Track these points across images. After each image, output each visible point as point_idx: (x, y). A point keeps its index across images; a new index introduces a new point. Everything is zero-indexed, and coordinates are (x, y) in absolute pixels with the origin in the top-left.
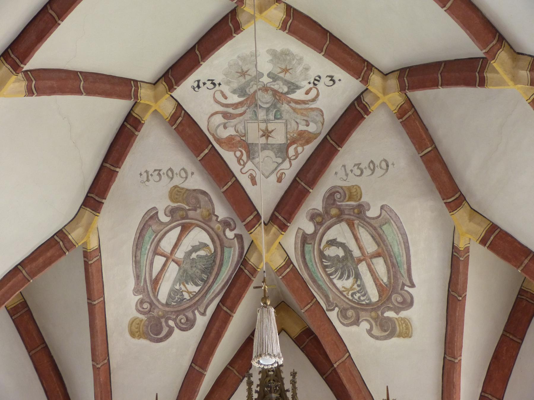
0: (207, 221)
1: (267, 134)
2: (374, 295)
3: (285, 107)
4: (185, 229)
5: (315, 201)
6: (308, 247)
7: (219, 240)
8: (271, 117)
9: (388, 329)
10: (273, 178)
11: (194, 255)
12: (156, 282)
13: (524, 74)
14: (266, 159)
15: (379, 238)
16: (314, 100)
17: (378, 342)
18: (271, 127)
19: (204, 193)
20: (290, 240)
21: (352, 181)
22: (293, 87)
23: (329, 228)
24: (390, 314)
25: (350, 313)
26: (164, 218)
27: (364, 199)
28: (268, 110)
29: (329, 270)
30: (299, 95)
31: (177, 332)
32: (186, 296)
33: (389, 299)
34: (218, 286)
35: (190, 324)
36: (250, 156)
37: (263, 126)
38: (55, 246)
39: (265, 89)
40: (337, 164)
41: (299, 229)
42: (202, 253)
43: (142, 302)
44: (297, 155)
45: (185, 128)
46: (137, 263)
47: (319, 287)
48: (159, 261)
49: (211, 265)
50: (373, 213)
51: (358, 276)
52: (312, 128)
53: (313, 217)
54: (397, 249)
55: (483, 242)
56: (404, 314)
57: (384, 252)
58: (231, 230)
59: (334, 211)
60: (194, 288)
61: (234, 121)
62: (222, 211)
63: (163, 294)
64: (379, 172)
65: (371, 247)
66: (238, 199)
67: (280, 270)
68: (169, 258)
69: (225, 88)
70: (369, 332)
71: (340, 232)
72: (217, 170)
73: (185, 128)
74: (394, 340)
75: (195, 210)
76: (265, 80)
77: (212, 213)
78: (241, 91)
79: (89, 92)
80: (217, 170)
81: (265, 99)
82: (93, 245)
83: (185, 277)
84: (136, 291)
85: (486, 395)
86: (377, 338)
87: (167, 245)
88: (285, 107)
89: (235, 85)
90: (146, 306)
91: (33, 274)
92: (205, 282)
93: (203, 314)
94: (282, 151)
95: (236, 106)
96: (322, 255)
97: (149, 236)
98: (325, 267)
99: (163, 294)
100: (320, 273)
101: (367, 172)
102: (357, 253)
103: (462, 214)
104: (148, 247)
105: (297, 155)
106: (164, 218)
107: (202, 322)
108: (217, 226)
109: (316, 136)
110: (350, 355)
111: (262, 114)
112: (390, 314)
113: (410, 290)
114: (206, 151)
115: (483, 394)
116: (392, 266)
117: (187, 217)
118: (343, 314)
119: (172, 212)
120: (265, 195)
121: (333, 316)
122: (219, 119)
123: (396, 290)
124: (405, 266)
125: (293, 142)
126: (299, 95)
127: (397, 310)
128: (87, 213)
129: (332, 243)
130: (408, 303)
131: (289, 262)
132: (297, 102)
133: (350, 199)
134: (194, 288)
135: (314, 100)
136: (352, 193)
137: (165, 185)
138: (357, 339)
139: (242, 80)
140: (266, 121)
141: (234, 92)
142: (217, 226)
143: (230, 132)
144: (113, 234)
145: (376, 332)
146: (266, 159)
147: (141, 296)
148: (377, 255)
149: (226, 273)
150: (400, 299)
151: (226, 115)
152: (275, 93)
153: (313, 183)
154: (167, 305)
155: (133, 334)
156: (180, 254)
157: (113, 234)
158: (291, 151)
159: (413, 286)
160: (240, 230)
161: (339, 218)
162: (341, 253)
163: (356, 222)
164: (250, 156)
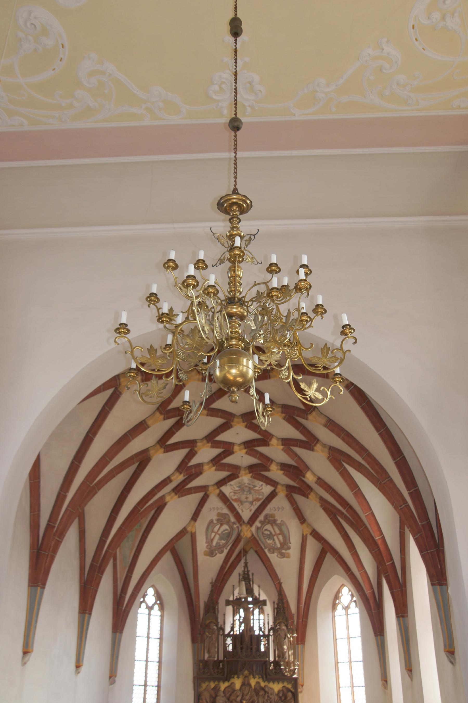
0: (228, 523)
1: (247, 498)
2: (279, 545)
3: (252, 491)
4: (222, 525)
5: (261, 517)
6: (259, 531)
7: (232, 528)
8: (248, 493)
9: (283, 556)
10: (248, 510)
11: (224, 532)
12: (212, 540)
13: (318, 500)
14: (247, 505)
15: (280, 529)
16: (261, 489)
17: (280, 559)
18: (248, 496)
19: (227, 514)
20: (253, 529)
21: (273, 512)
22: (255, 486)
23: (265, 525)
24: (283, 551)
25: (271, 550)
26: (215, 522)
27: (276, 518)
28: (247, 492)
29: (265, 538)
30: (256, 488)
31: (218, 555)
32: (221, 544)
33: (283, 547)
34: (231, 541)
35: (222, 552)
36: (242, 504)
37: (246, 496)
38: (183, 533)
39: (246, 487)
40: (268, 507)
41: (256, 526)
42: (226, 532)
43: (208, 546)
44: (256, 504)
45: (223, 498)
46: (207, 535)
47: (262, 542)
48: (213, 534)
49: (229, 535)
50: (279, 522)
51: (274, 540)
52: (261, 497)
53: (261, 522)
54: (286, 533)
55: (311, 534)
56: (288, 551)
57: (282, 533)
58: (236, 525)
59: (267, 521)
60: (223, 542)
61: (237, 495)
62: (233, 519)
63: (214, 543)
64: (280, 510)
65: (278, 532)
66: (238, 517)
67: (250, 538)
68: (216, 533)
69: (235, 486)
70: (277, 556)
71: (268, 527)
72: (232, 508)
73: (223, 498)
74: (285, 559)
75: (224, 519)
76: (246, 485)
77: (229, 520)
78: (239, 487)
79: (195, 492)
80: (232, 508)
81: (247, 489)
82: (194, 531)
83: (221, 539)
84: (206, 542)
86: (280, 558)
87: (216, 529)
88: (252, 491)
89: (237, 485)
90: (209, 547)
91: (177, 541)
92: (227, 540)
93: (226, 549)
94: (251, 503)
95: (238, 490)
96: (263, 533)
97: (210, 528)
98: (264, 537)
99: (214, 543)
100: (263, 539)
101: (277, 510)
102: (273, 533)
103: (305, 525)
104: (210, 530)
105: (256, 504)
106: (215, 522)
107: (226, 551)
108: (231, 524)
109: (261, 499)
111: (245, 493)
112: (283, 551)
113: (290, 545)
114: (228, 503)
116: (284, 537)
117: (221, 521)
118: (269, 550)
119: (218, 520)
120: (246, 515)
121: (266, 551)
122: (232, 494)
123: (285, 544)
124: (288, 538)
125: (254, 500)
126: (256, 488)
127: (286, 550)
128: (193, 522)
129: (266, 530)
130: (289, 548)
131: (253, 535)
132: (256, 490)
133: (272, 517)
134: (223, 542)
135: (261, 489)
136: (272, 516)
137: (216, 512)
138: (273, 558)
139: (239, 485)
140: (247, 495)
141: (237, 487)
142: (231, 524)
143: (235, 497)
144: (200, 528)
145: (279, 556)
146: (247, 505)
147: (207, 544)
148: (279, 534)
149: (234, 537)
150: (286, 547)
151: (234, 493)
152: (249, 488)
153: (260, 513)
154: (215, 546)
155: (205, 555)
156: (220, 532)
157: (200, 528)
158: (254, 503)
159: (290, 543)
160: (238, 525)
161: (268, 523)
162: (269, 533)
163: (274, 524)
164: (242, 504)
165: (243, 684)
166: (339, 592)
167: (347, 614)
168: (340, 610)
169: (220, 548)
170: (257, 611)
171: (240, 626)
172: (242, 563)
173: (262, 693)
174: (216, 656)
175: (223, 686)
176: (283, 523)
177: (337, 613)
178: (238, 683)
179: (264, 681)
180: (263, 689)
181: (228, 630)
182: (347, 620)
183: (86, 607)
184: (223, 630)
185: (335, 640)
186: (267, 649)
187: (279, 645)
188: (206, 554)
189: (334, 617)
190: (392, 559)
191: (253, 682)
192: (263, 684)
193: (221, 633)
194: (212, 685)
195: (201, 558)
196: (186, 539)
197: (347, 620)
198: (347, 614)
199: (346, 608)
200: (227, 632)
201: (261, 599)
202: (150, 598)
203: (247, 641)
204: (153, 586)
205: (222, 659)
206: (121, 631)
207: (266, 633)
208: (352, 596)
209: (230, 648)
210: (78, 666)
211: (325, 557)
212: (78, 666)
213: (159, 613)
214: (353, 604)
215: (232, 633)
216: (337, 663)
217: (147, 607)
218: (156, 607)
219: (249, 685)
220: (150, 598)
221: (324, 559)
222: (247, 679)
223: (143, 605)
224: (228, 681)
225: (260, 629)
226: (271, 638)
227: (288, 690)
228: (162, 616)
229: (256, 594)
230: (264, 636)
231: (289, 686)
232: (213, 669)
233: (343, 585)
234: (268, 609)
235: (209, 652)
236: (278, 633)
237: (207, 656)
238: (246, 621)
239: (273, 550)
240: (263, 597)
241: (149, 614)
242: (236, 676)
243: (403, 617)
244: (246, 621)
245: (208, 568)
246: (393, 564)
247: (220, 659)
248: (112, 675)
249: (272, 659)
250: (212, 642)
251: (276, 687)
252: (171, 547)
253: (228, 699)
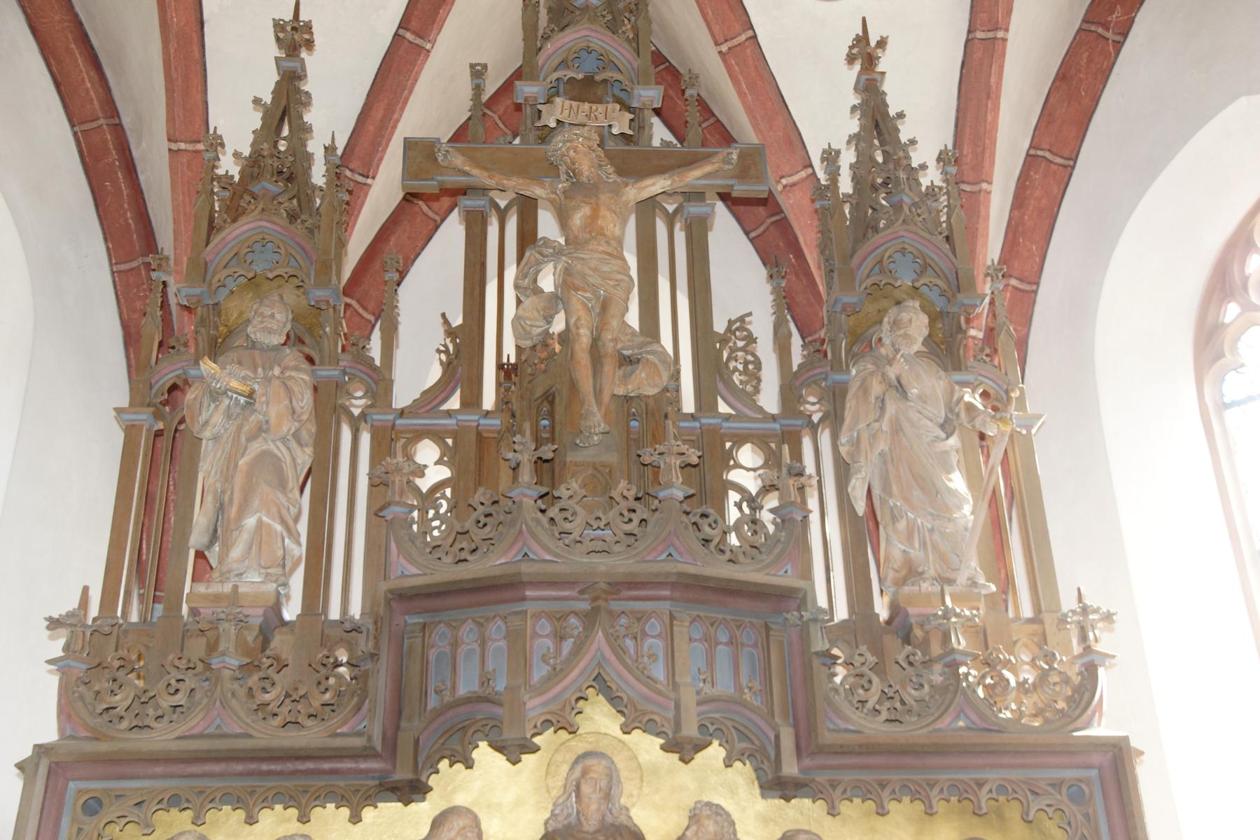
85: (1040, 153)
110: (755, 37)
115: (1032, 152)
174: (297, 581)
177: (1233, 386)
179: (777, 786)
193: (357, 405)
205: (356, 610)
207: (769, 399)
211: (1125, 30)
215: (454, 403)
221: (1119, 46)
222: (598, 767)
224: (413, 790)
232: (249, 668)
236: (892, 372)
242: (483, 753)
247: (334, 614)
250: (256, 447)
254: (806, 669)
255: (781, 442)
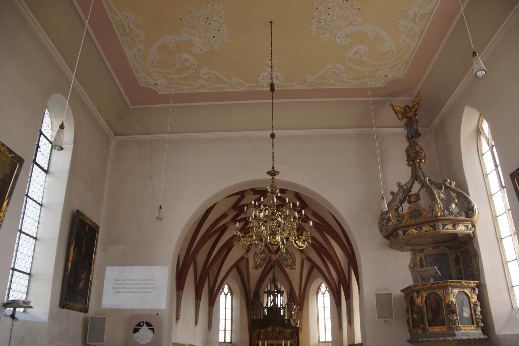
2: (290, 264)
4: (261, 254)
7: (267, 256)
9: (292, 269)
12: (257, 262)
20: (277, 256)
35: (262, 267)
38: (242, 258)
46: (254, 259)
49: (265, 259)
57: (292, 258)
62: (267, 251)
63: (258, 263)
65: (290, 257)
83: (261, 261)
99: (258, 263)
103: (303, 254)
107: (263, 267)
116: (293, 260)
123: (293, 263)
130: (295, 265)
138: (287, 270)
144: (250, 256)
149: (267, 260)
165: (273, 330)
166: (320, 286)
167: (324, 297)
168: (320, 295)
169: (260, 265)
170: (279, 295)
171: (271, 303)
172: (272, 271)
173: (281, 334)
175: (263, 331)
176: (292, 253)
177: (319, 296)
178: (270, 329)
180: (282, 332)
181: (265, 305)
182: (324, 300)
183: (198, 297)
184: (263, 305)
185: (318, 308)
186: (284, 313)
187: (290, 312)
188: (253, 268)
189: (317, 298)
190: (344, 273)
191: (277, 329)
192: (282, 330)
194: (258, 330)
195: (251, 270)
196: (244, 261)
197: (324, 300)
198: (324, 297)
199: (324, 294)
200: (264, 306)
201: (282, 290)
202: (226, 289)
203: (274, 309)
204: (227, 284)
206: (213, 306)
208: (326, 288)
209: (266, 314)
210: (196, 323)
212: (196, 323)
213: (230, 297)
214: (327, 292)
216: (318, 319)
217: (225, 294)
218: (229, 294)
219: (276, 330)
220: (226, 289)
223: (223, 293)
225: (281, 305)
226: (286, 309)
227: (294, 332)
228: (232, 299)
229: (279, 287)
230: (283, 308)
231: (295, 330)
233: (322, 283)
234: (285, 295)
235: (256, 315)
237: (255, 317)
238: (274, 301)
239: (287, 266)
240: (282, 289)
241: (226, 297)
243: (348, 300)
244: (274, 301)
245: (255, 274)
246: (345, 276)
248: (210, 326)
249: (286, 318)
251: (289, 331)
252: (236, 265)
253: (266, 337)
254: (284, 322)
255: (284, 308)
